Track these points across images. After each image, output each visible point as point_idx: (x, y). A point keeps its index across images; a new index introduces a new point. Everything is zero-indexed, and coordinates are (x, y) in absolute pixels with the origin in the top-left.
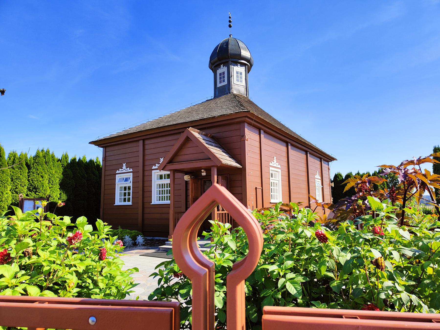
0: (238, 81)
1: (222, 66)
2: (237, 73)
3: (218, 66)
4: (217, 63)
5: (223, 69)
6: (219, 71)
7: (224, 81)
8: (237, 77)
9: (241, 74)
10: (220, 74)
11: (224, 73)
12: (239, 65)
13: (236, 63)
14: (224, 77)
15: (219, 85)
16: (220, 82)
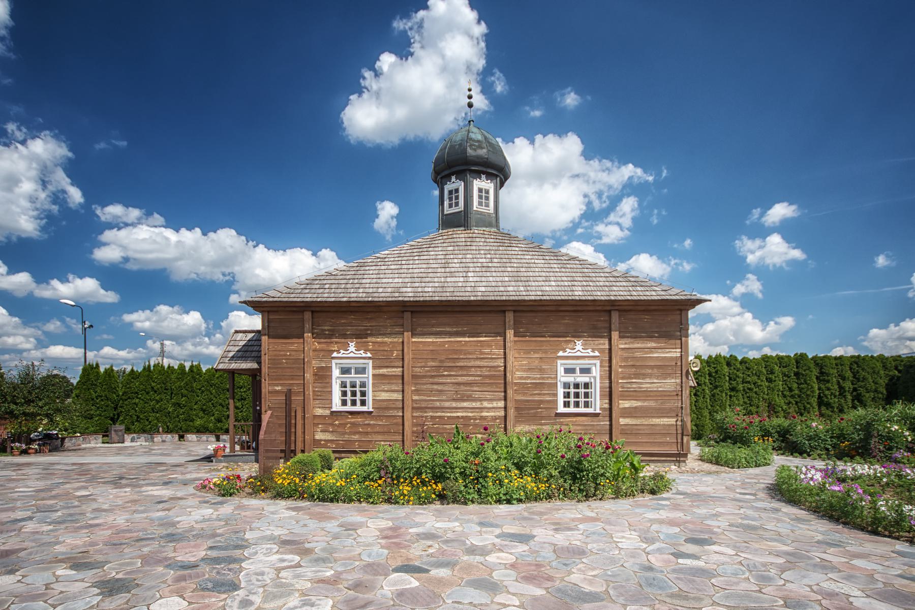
0: (480, 204)
1: (453, 179)
2: (480, 190)
3: (448, 177)
4: (446, 173)
5: (455, 184)
6: (448, 187)
7: (457, 204)
8: (480, 197)
9: (487, 192)
10: (450, 192)
11: (457, 191)
12: (483, 176)
13: (478, 174)
14: (457, 198)
15: (447, 210)
16: (450, 206)
